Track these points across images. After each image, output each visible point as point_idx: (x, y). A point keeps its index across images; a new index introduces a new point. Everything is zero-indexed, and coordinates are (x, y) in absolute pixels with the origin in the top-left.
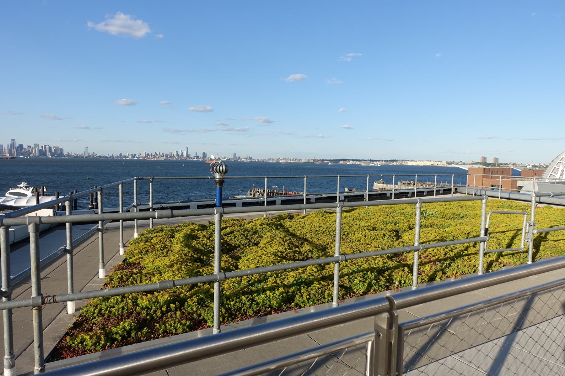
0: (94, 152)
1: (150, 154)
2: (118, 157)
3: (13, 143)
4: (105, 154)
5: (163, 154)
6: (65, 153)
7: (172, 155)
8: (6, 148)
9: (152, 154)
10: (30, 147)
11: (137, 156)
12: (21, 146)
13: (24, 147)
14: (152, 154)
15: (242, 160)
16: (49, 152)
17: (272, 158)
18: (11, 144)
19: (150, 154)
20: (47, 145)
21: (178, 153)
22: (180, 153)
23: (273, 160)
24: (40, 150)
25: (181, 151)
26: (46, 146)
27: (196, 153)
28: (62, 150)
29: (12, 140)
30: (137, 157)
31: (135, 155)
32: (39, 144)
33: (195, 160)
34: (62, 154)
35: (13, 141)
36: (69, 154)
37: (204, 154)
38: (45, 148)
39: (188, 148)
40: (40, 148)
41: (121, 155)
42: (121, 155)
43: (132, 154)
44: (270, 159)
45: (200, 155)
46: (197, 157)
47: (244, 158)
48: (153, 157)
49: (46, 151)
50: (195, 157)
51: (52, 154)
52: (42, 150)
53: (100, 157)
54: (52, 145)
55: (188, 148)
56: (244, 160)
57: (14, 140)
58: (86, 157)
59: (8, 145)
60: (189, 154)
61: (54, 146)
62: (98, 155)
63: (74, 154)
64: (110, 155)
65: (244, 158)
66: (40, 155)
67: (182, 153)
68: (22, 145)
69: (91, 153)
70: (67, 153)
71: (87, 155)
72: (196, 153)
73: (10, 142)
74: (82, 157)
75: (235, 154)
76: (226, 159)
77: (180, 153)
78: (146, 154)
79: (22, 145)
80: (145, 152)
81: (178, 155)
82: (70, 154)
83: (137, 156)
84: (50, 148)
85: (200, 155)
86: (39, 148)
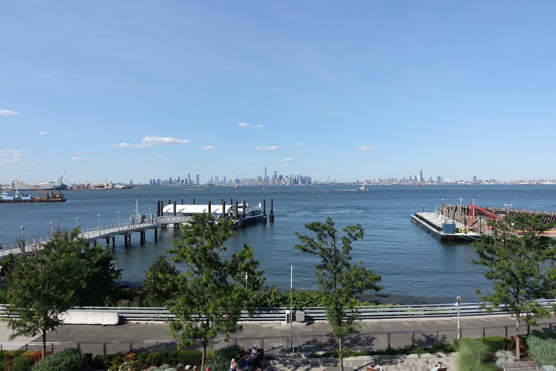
0: (335, 180)
1: (384, 180)
2: (354, 183)
3: (276, 174)
4: (345, 182)
5: (396, 179)
6: (313, 181)
7: (406, 180)
8: (271, 179)
9: (385, 180)
10: (287, 177)
11: (372, 182)
12: (281, 177)
13: (283, 177)
14: (385, 180)
15: (484, 182)
16: (301, 181)
17: (523, 180)
18: (274, 175)
19: (384, 180)
20: (299, 175)
21: (412, 178)
22: (413, 178)
23: (525, 182)
24: (294, 179)
25: (415, 175)
26: (298, 175)
27: (431, 177)
28: (310, 178)
29: (275, 172)
30: (372, 183)
31: (370, 181)
32: (293, 175)
33: (430, 184)
34: (310, 182)
35: (276, 173)
36: (315, 182)
37: (439, 177)
38: (298, 177)
39: (421, 172)
40: (294, 178)
41: (357, 181)
42: (357, 181)
43: (368, 180)
44: (521, 181)
45: (435, 179)
46: (432, 182)
47: (486, 181)
48: (387, 182)
49: (298, 180)
50: (429, 181)
51: (302, 183)
52: (296, 179)
53: (339, 184)
54: (304, 175)
55: (421, 172)
56: (487, 183)
57: (277, 172)
58: (328, 184)
59: (272, 176)
60: (423, 178)
61: (304, 175)
62: (338, 182)
63: (319, 182)
64: (349, 182)
65: (486, 181)
66: (294, 184)
67: (416, 178)
68: (282, 176)
69: (333, 180)
70: (314, 181)
71: (329, 182)
72: (431, 177)
73: (274, 174)
74: (325, 184)
75: (475, 177)
76: (463, 183)
77: (413, 178)
78: (380, 179)
79: (282, 176)
80: (379, 178)
81: (411, 180)
82: (317, 182)
83: (372, 182)
84: (301, 177)
85: (435, 179)
86: (293, 177)
